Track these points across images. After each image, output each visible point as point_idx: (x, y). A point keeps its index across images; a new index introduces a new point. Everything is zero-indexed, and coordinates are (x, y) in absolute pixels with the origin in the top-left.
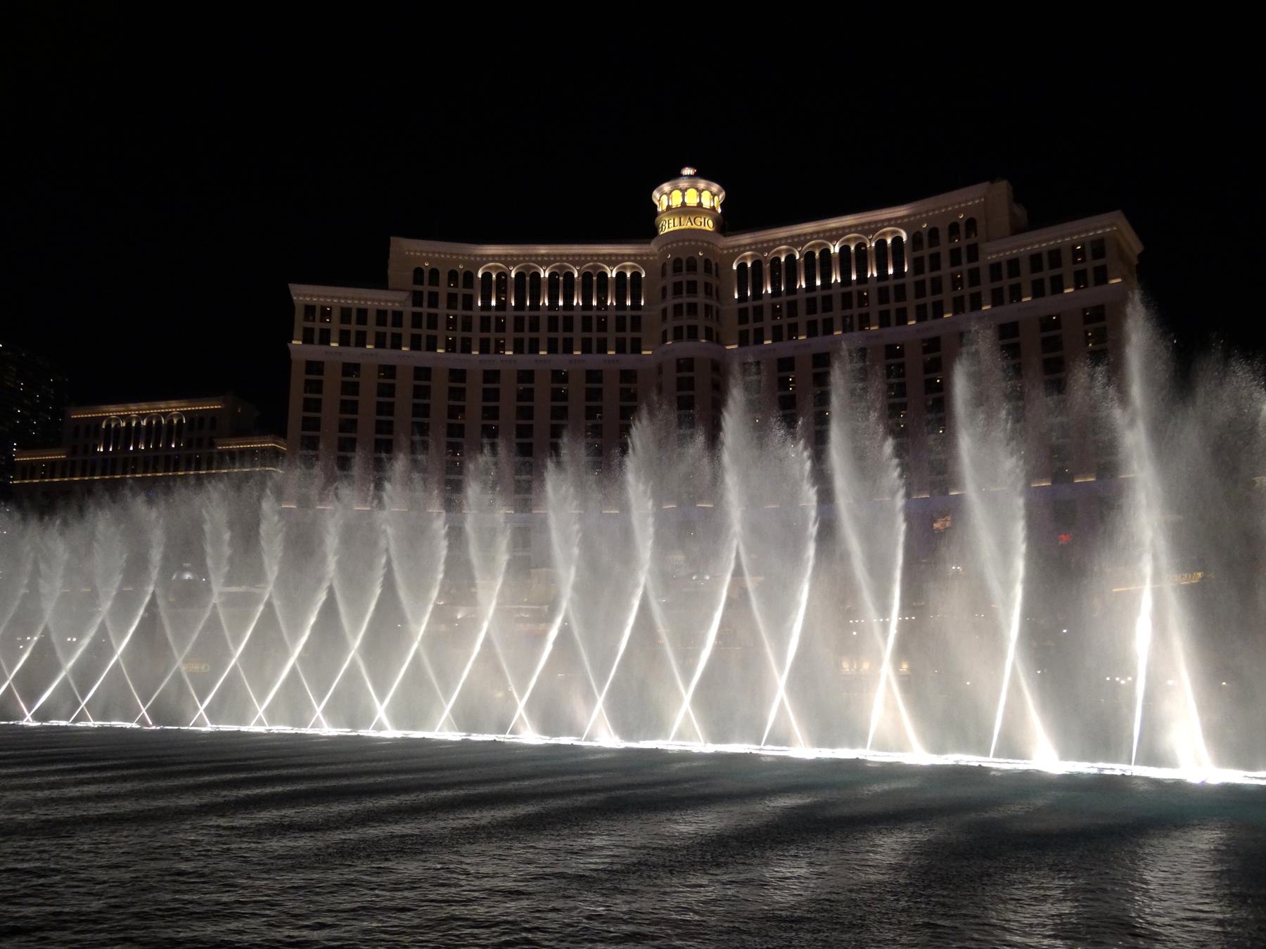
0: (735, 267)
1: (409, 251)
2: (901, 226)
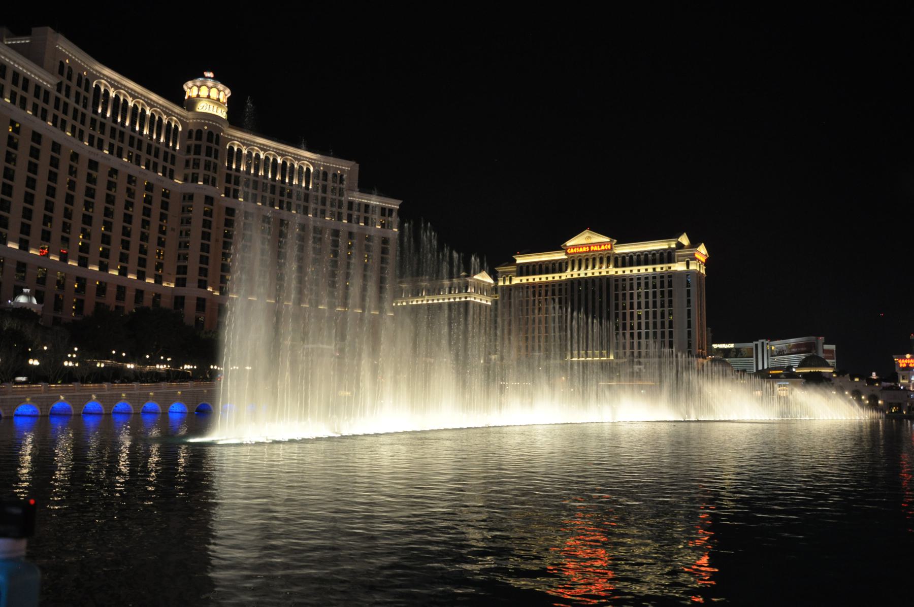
0: (228, 148)
1: (59, 45)
2: (313, 164)
